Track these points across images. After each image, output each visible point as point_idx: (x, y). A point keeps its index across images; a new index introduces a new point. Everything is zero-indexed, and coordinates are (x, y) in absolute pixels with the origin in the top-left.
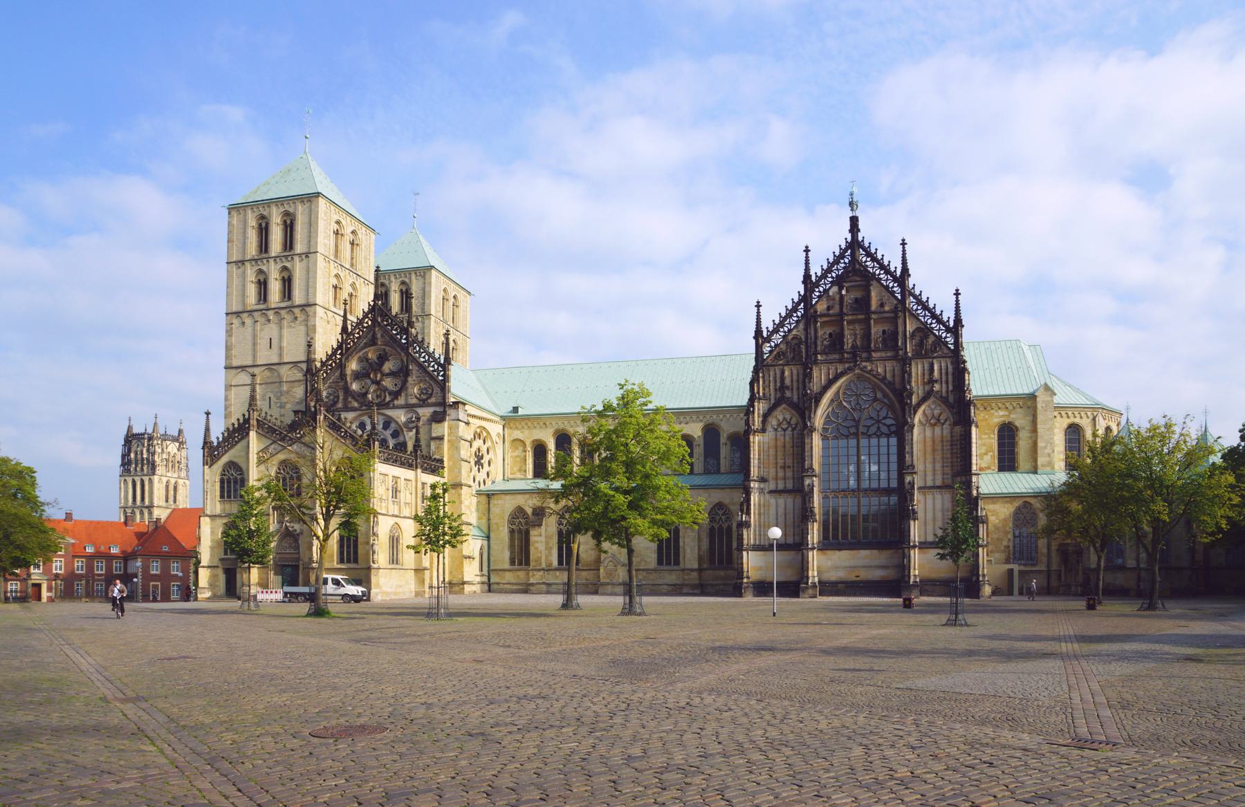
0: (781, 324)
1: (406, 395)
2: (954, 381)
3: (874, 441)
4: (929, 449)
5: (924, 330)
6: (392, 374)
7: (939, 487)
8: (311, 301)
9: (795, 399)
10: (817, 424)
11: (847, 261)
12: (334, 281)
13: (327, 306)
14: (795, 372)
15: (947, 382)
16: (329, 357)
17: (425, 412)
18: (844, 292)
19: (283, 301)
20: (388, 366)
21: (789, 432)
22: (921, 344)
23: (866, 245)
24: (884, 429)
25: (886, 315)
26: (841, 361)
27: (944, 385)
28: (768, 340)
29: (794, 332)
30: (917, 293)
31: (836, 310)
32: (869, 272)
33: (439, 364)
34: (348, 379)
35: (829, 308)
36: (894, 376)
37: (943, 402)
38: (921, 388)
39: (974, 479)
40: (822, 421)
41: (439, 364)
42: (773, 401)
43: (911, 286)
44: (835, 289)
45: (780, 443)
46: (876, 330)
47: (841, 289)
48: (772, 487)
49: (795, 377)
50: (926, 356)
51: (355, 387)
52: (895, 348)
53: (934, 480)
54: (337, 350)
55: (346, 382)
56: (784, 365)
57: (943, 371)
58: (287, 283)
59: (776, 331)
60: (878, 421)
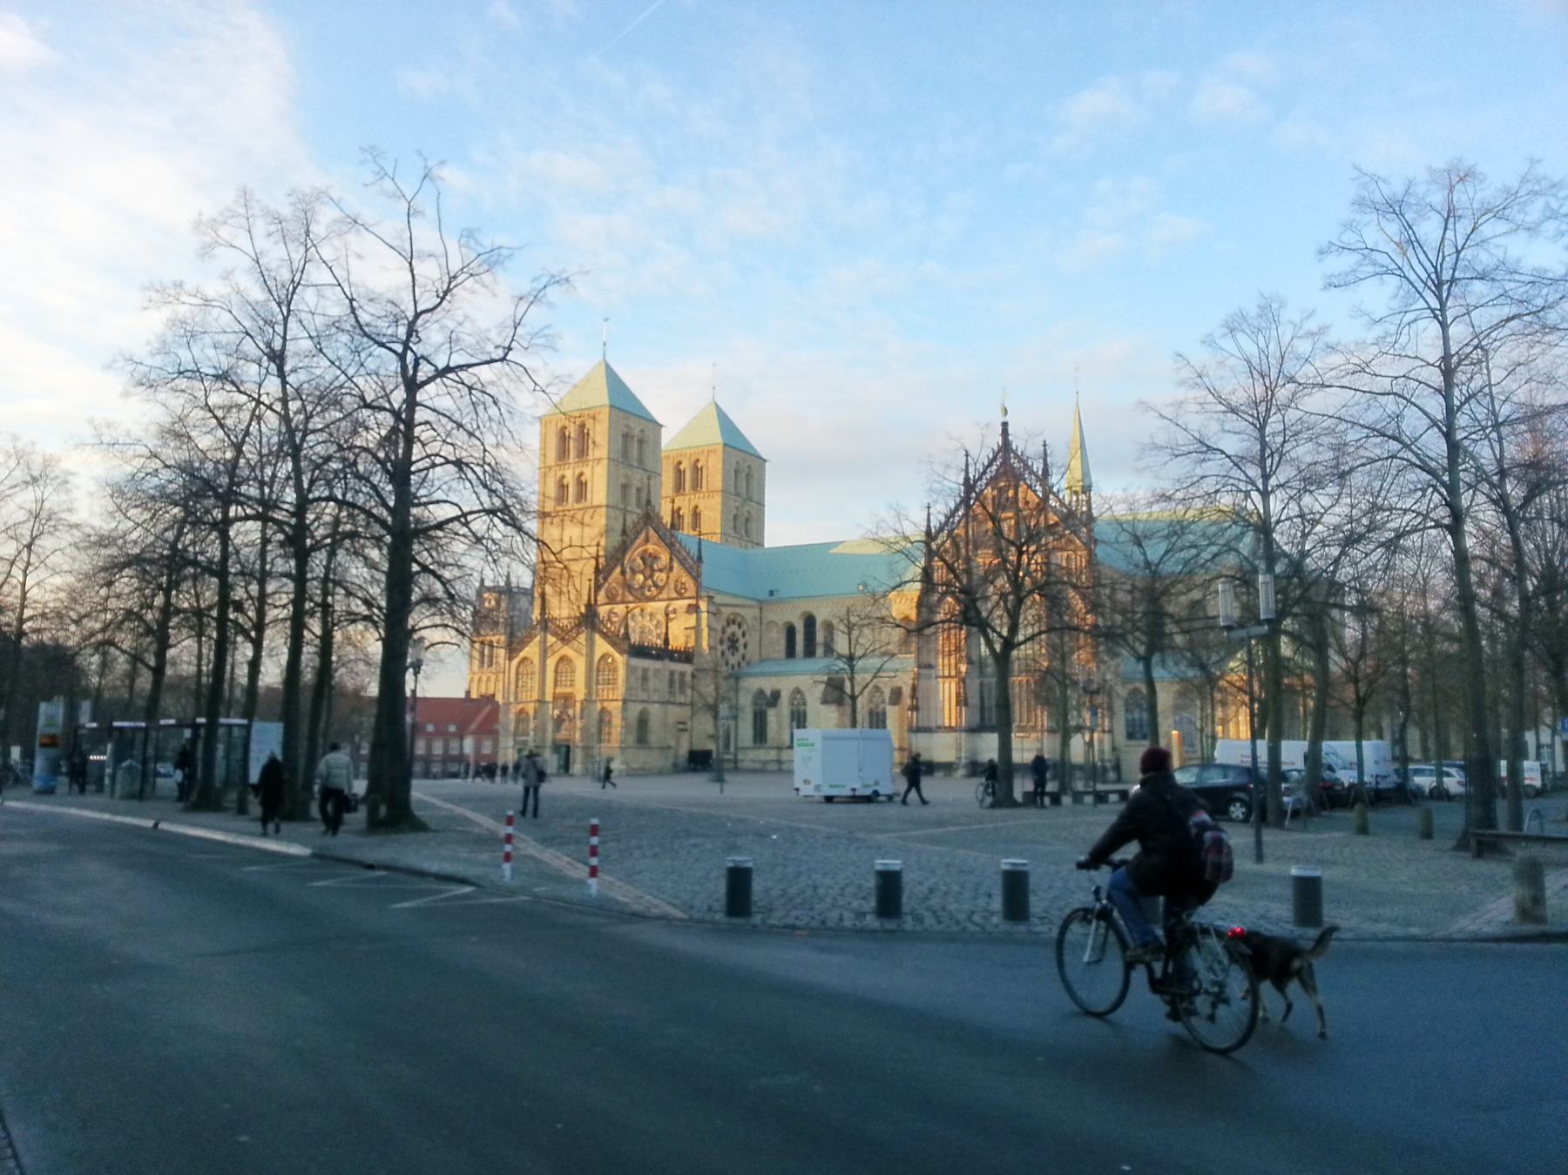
6: (661, 571)
44: (989, 489)
58: (582, 485)
59: (941, 529)
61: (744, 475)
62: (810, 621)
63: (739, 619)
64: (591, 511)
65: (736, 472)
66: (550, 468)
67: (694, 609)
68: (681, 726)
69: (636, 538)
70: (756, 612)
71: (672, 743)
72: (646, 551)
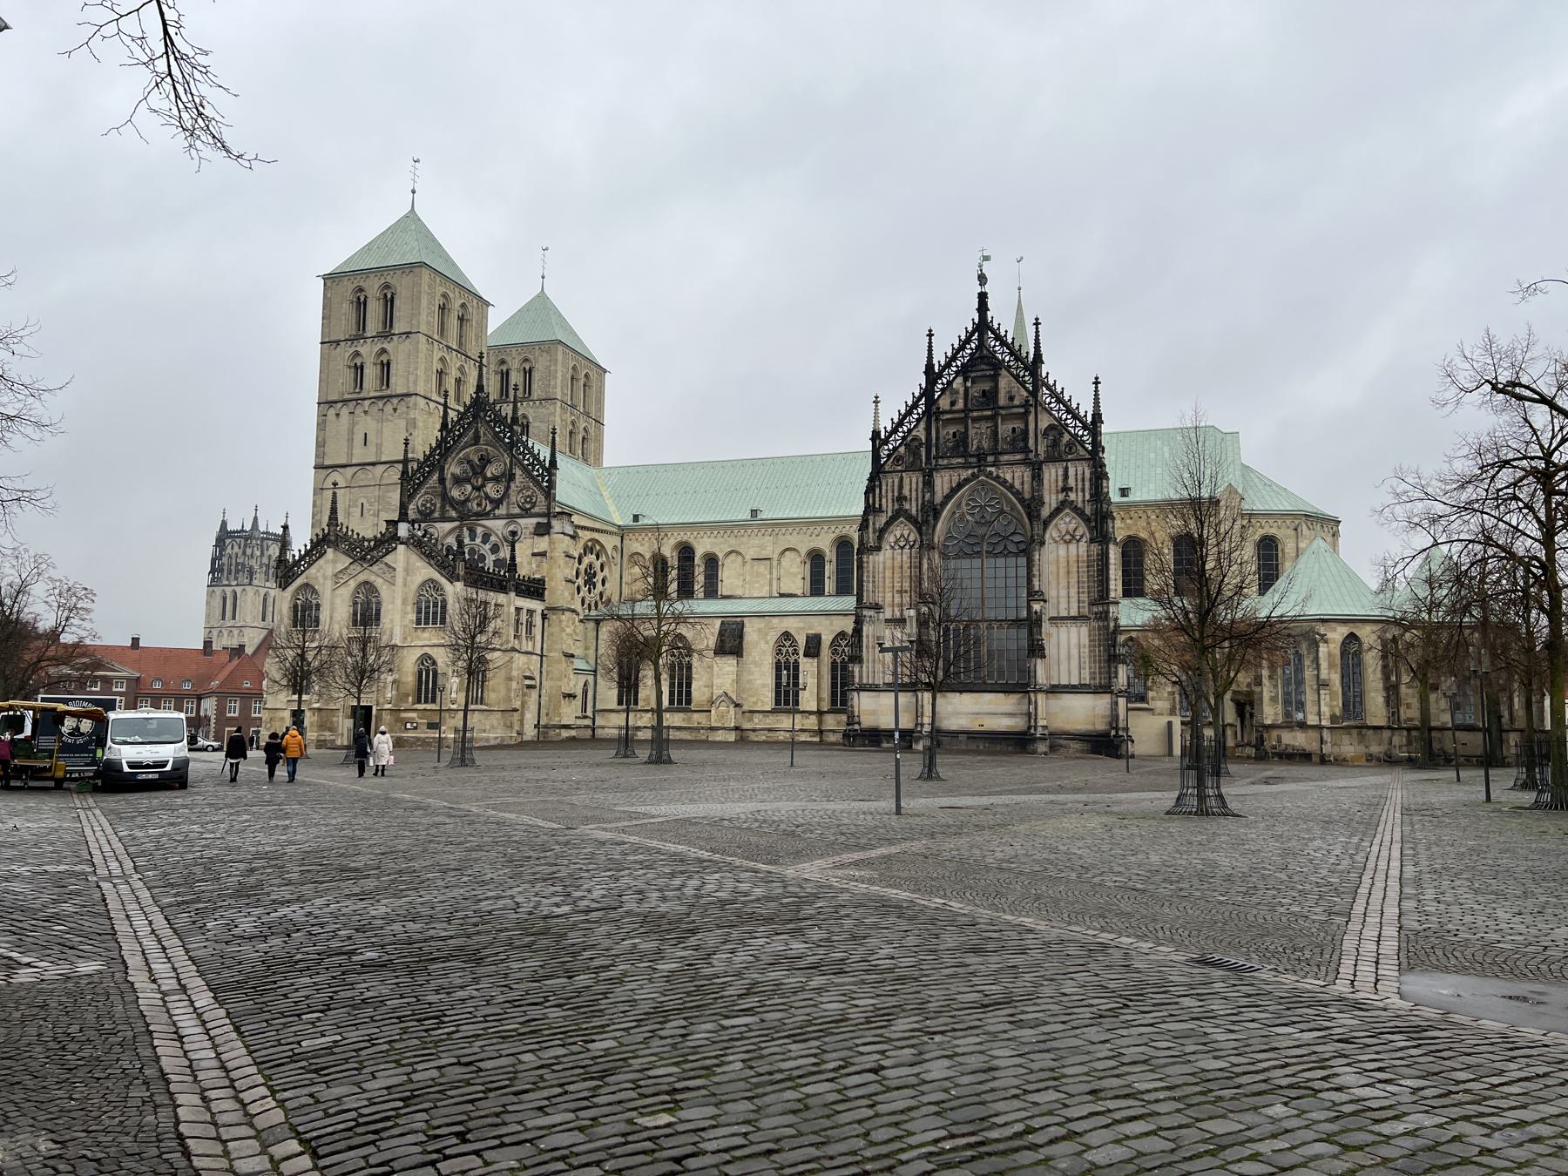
0: (901, 423)
1: (508, 504)
2: (1091, 489)
3: (1001, 561)
4: (1062, 571)
5: (1057, 429)
6: (496, 479)
7: (1074, 618)
8: (412, 391)
9: (914, 512)
10: (936, 540)
11: (973, 346)
12: (440, 366)
13: (429, 395)
14: (914, 480)
15: (1083, 490)
16: (427, 458)
17: (529, 523)
18: (969, 384)
19: (381, 390)
20: (490, 471)
21: (906, 550)
22: (1055, 444)
23: (996, 326)
24: (1012, 548)
25: (1015, 410)
26: (965, 466)
27: (1080, 494)
28: (886, 441)
29: (914, 433)
30: (1051, 383)
31: (960, 405)
32: (997, 359)
33: (543, 467)
34: (448, 484)
35: (953, 403)
36: (1023, 483)
37: (1079, 515)
38: (1054, 497)
39: (1112, 609)
40: (942, 539)
41: (543, 467)
42: (890, 514)
43: (1044, 375)
44: (960, 380)
45: (897, 564)
46: (1005, 429)
47: (965, 380)
48: (888, 615)
49: (914, 486)
50: (1059, 459)
51: (455, 493)
52: (1026, 450)
53: (1068, 609)
54: (435, 450)
55: (445, 488)
56: (901, 471)
57: (1079, 477)
58: (386, 367)
59: (895, 431)
60: (1005, 538)
61: (582, 383)
62: (686, 552)
63: (598, 547)
64: (395, 401)
65: (572, 378)
66: (338, 342)
67: (543, 530)
68: (528, 682)
69: (460, 436)
70: (616, 541)
71: (517, 704)
72: (477, 451)
